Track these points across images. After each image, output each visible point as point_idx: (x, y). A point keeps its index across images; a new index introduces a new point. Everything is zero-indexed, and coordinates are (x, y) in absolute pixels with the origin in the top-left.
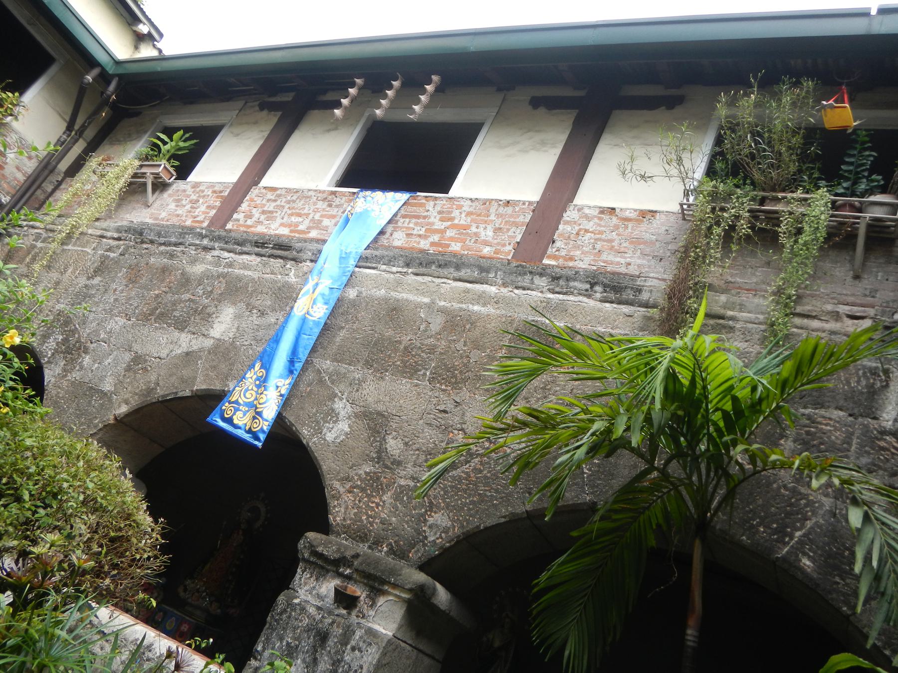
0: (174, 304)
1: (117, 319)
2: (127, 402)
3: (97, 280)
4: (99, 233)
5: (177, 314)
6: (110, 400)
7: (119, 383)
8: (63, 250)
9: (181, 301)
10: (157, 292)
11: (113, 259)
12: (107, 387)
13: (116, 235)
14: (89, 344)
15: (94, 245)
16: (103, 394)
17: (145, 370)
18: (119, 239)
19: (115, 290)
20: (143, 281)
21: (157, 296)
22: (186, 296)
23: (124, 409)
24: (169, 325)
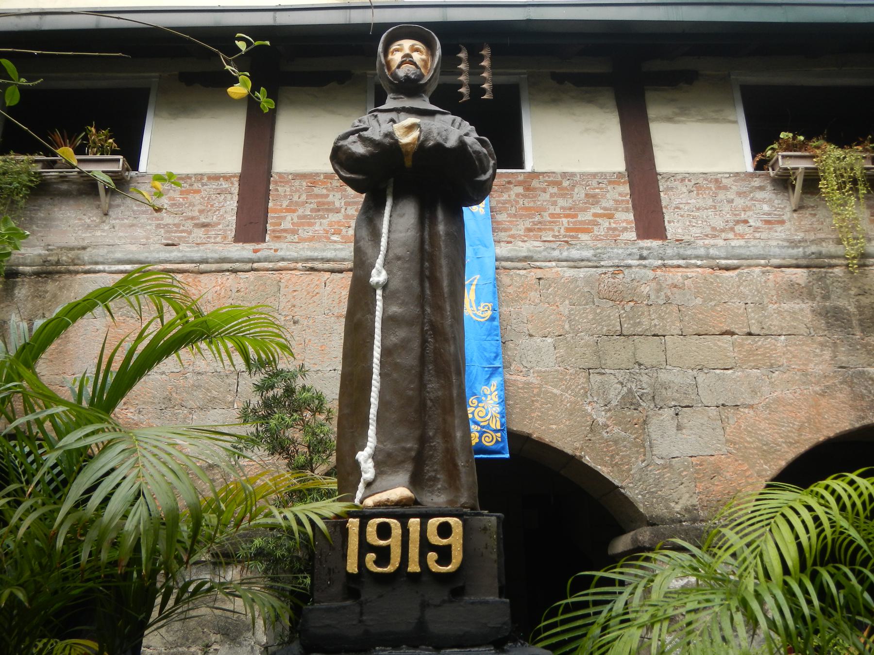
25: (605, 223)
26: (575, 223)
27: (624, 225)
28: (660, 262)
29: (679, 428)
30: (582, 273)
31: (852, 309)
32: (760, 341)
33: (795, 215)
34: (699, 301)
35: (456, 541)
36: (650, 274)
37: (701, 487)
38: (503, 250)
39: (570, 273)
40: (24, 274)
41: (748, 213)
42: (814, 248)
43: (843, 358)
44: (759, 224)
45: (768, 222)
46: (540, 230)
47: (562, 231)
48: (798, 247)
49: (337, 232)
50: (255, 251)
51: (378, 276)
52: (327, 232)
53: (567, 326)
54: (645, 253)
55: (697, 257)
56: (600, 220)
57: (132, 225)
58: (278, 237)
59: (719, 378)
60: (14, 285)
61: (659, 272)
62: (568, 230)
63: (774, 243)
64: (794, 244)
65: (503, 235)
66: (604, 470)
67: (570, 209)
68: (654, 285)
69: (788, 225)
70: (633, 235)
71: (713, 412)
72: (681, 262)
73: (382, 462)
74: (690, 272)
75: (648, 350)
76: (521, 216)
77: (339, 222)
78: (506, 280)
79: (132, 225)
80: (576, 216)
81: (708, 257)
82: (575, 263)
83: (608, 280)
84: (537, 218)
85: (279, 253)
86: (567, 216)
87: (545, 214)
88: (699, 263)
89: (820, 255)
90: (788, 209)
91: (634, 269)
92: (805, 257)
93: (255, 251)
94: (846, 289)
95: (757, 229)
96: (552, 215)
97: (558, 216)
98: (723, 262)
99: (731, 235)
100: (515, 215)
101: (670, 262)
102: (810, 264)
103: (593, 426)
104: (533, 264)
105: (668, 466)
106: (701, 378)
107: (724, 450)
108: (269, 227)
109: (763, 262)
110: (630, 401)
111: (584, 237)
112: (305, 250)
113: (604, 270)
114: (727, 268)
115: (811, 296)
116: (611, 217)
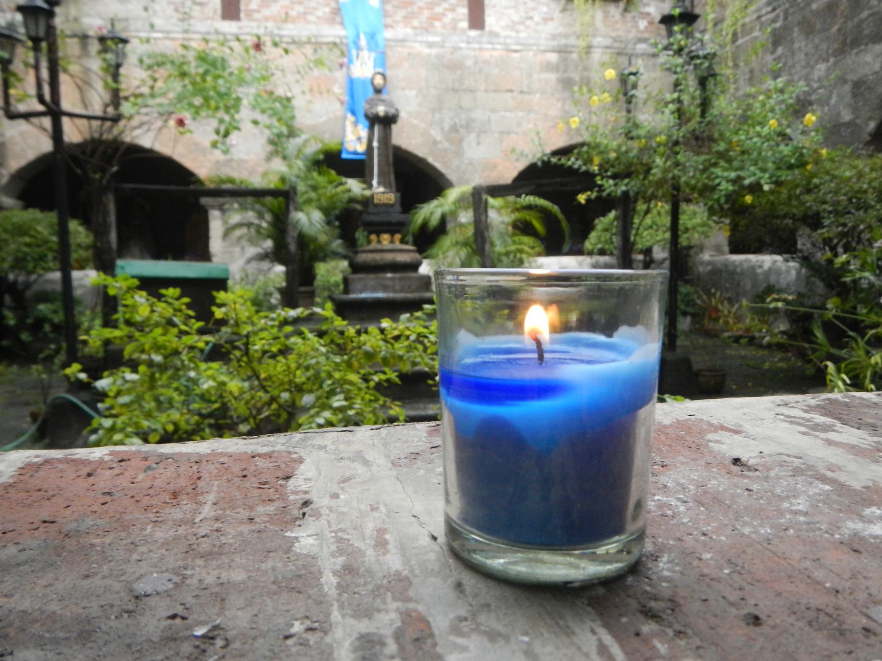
0: (859, 26)
1: (818, 66)
2: (870, 119)
3: (780, 50)
4: (755, 16)
5: (867, 32)
6: (855, 125)
7: (855, 110)
8: (737, 47)
9: (862, 21)
10: (836, 27)
11: (780, 28)
12: (846, 116)
13: (769, 9)
14: (808, 98)
15: (758, 27)
16: (848, 124)
17: (869, 88)
18: (774, 10)
19: (800, 48)
20: (818, 26)
21: (839, 30)
22: (865, 14)
23: (872, 125)
24: (867, 44)
25: (450, 15)
28: (477, 46)
29: (479, 143)
30: (434, 51)
36: (472, 53)
38: (389, 34)
39: (426, 51)
51: (375, 144)
53: (423, 84)
54: (470, 40)
63: (543, 35)
64: (554, 37)
65: (389, 21)
66: (438, 165)
70: (465, 24)
71: (497, 135)
73: (379, 183)
74: (495, 53)
75: (466, 100)
78: (389, 53)
80: (432, 9)
82: (430, 45)
86: (428, 9)
89: (566, 46)
95: (537, 23)
98: (514, 47)
99: (521, 27)
102: (562, 51)
103: (435, 143)
105: (471, 164)
109: (535, 48)
110: (454, 129)
111: (437, 24)
114: (515, 51)
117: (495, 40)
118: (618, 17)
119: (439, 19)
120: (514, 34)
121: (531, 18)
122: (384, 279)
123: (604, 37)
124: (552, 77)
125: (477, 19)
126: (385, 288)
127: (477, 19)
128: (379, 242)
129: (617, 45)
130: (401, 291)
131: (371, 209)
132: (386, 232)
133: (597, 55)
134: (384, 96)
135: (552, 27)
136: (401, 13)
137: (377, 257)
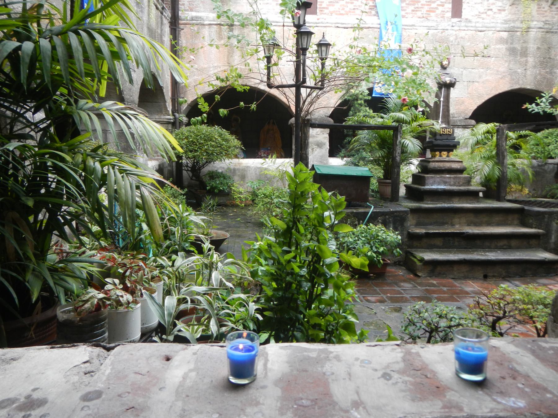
25: (441, 8)
26: (430, 8)
27: (448, 10)
28: (458, 28)
31: (519, 48)
32: (486, 59)
33: (510, 7)
34: (469, 44)
35: (451, 131)
36: (454, 33)
37: (457, 107)
38: (405, 21)
40: (235, 25)
41: (494, 6)
42: (512, 25)
43: (511, 66)
44: (496, 11)
45: (499, 10)
46: (417, 11)
47: (425, 12)
48: (507, 24)
49: (343, 9)
50: (318, 19)
52: (339, 9)
54: (454, 24)
55: (472, 27)
56: (439, 7)
57: (267, 4)
58: (322, 11)
59: (470, 72)
60: (233, 29)
61: (457, 32)
62: (427, 11)
63: (499, 21)
64: (506, 22)
67: (429, 2)
68: (454, 37)
69: (506, 12)
70: (449, 14)
71: (465, 83)
72: (466, 28)
73: (442, 122)
74: (469, 33)
76: (410, 5)
77: (343, 5)
79: (267, 4)
80: (430, 5)
81: (475, 27)
83: (440, 35)
84: (416, 6)
85: (326, 21)
86: (428, 5)
87: (419, 4)
88: (472, 29)
89: (514, 27)
90: (508, 5)
91: (449, 31)
92: (509, 27)
93: (318, 19)
94: (519, 40)
96: (422, 5)
97: (424, 5)
98: (480, 29)
99: (484, 16)
100: (408, 4)
101: (461, 28)
104: (415, 28)
106: (464, 72)
107: (467, 96)
108: (318, 6)
109: (493, 29)
111: (432, 14)
112: (334, 19)
113: (438, 31)
115: (507, 43)
116: (443, 6)
117: (470, 24)
118: (547, 8)
119: (434, 12)
120: (480, 20)
121: (491, 10)
122: (445, 177)
123: (538, 21)
124: (503, 47)
125: (457, 11)
126: (445, 183)
127: (457, 11)
128: (440, 156)
129: (546, 26)
130: (454, 185)
131: (438, 137)
132: (445, 150)
133: (533, 34)
134: (448, 71)
135: (504, 16)
136: (412, 8)
137: (441, 165)
